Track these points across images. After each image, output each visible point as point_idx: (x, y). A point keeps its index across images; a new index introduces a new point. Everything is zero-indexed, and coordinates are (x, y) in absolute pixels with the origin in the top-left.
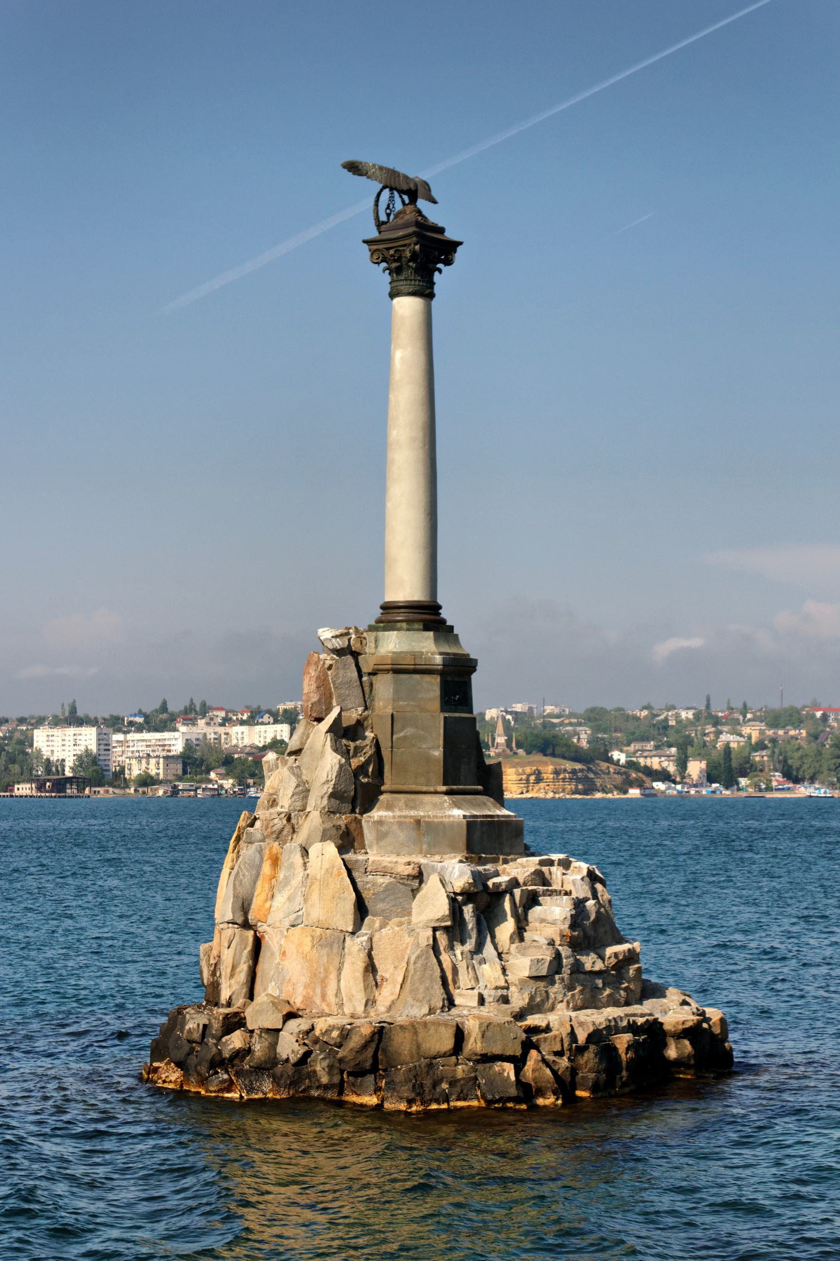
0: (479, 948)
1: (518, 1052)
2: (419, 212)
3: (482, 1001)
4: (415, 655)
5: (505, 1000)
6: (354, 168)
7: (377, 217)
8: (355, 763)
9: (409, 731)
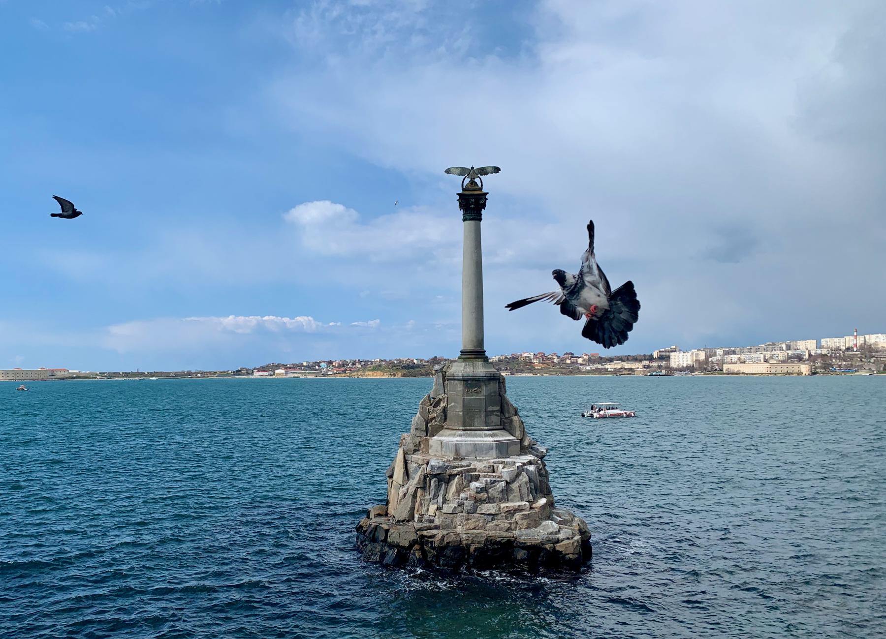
0: (436, 496)
1: (407, 545)
3: (420, 520)
5: (432, 521)
6: (448, 171)
8: (431, 416)
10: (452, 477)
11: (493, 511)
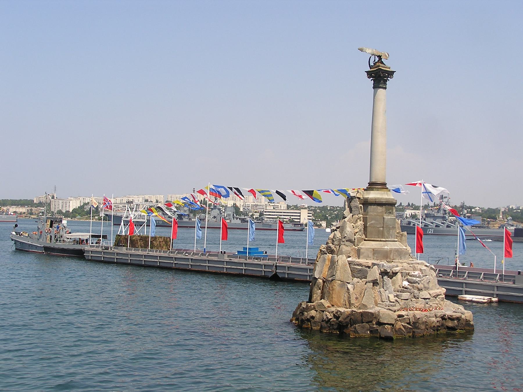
2: (382, 63)
4: (376, 199)
7: (369, 64)
9: (373, 222)
10: (395, 274)
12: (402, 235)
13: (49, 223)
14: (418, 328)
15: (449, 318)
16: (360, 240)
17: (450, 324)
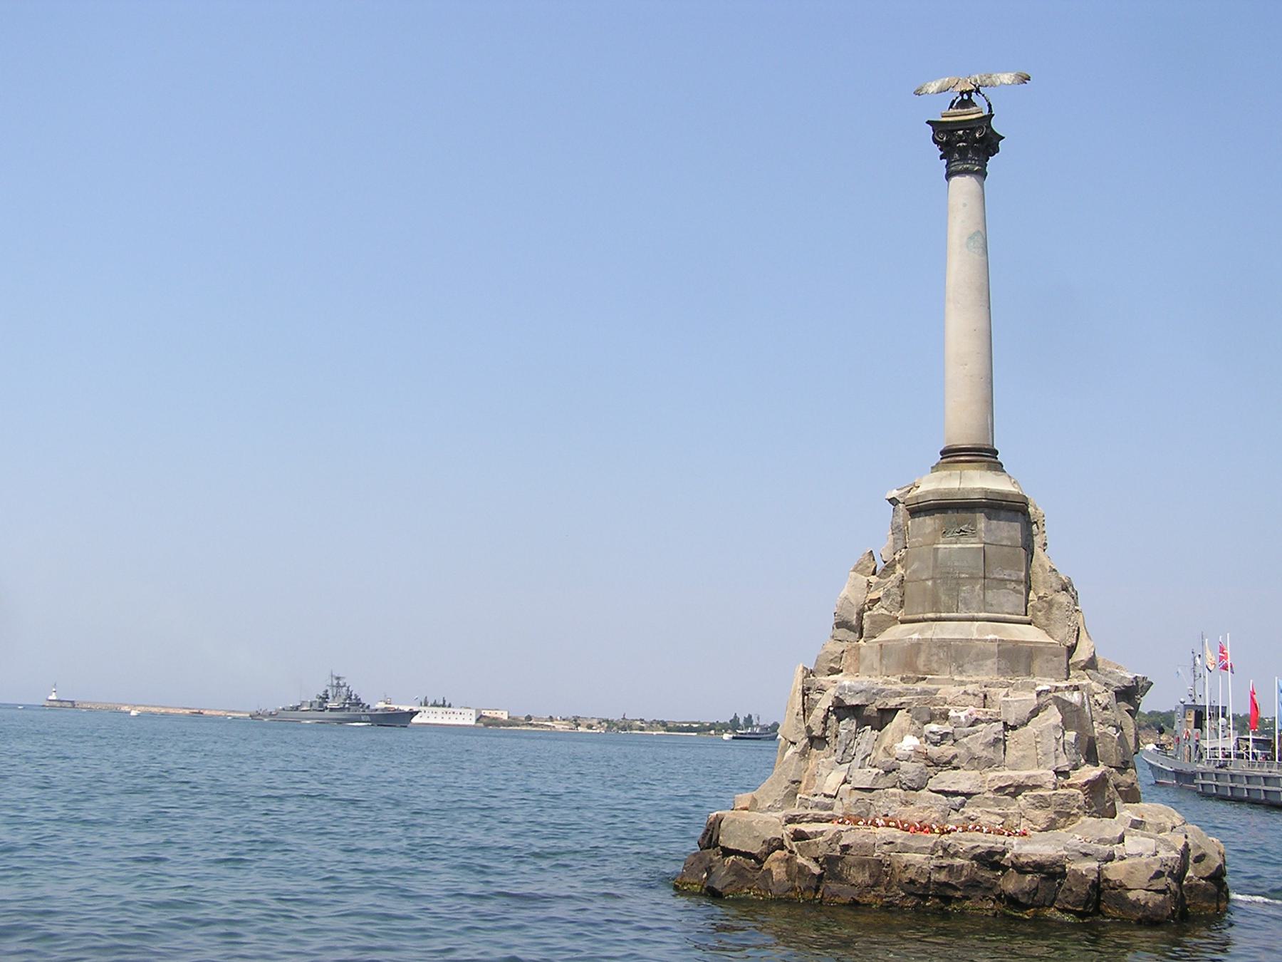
8: (874, 596)
9: (915, 566)
10: (886, 715)
11: (964, 787)
12: (1051, 604)
13: (1192, 718)
14: (838, 878)
15: (1014, 866)
16: (882, 624)
17: (1011, 884)
